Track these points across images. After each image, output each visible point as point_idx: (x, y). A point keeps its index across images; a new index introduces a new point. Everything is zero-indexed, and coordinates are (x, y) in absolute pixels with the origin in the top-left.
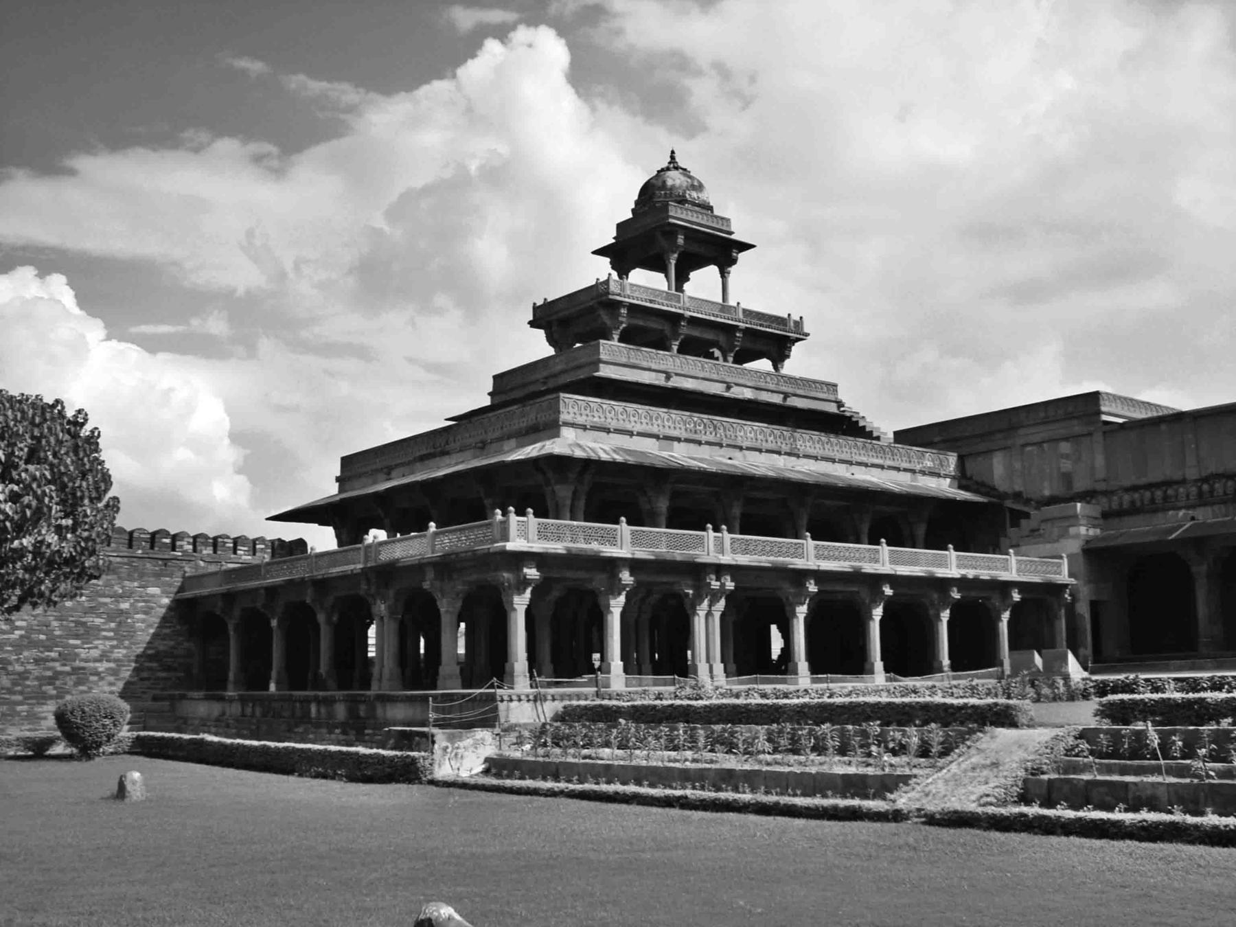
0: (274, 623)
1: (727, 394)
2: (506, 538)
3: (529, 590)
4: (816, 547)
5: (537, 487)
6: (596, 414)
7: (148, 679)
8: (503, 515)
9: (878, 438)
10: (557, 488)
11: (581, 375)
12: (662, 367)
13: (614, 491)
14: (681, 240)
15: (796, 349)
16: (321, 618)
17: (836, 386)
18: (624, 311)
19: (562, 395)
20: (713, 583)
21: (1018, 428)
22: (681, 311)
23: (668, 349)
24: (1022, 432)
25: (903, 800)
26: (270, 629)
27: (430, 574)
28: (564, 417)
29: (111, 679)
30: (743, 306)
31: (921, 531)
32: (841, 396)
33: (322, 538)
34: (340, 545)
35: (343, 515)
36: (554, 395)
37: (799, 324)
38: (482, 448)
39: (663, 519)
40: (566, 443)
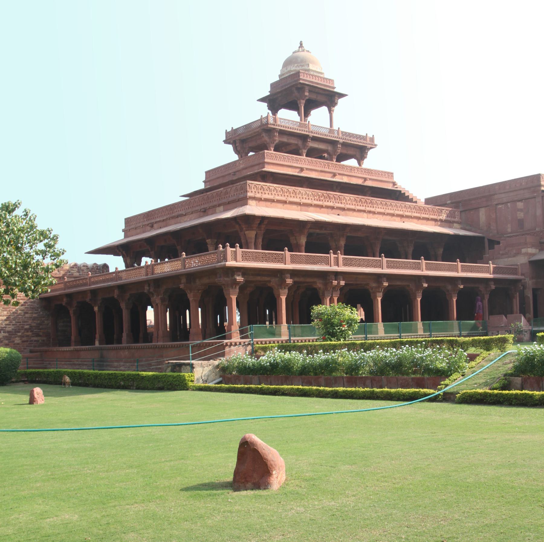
0: (96, 309)
1: (334, 180)
2: (225, 260)
3: (238, 287)
4: (387, 261)
5: (233, 232)
7: (27, 341)
8: (223, 248)
9: (416, 202)
10: (247, 232)
11: (256, 170)
13: (277, 234)
15: (370, 153)
16: (123, 306)
17: (392, 174)
19: (249, 182)
20: (334, 281)
21: (494, 195)
22: (307, 133)
23: (300, 155)
24: (496, 197)
25: (453, 384)
26: (94, 313)
27: (184, 280)
28: (249, 194)
29: (7, 342)
30: (341, 130)
31: (441, 251)
32: (395, 179)
33: (116, 263)
34: (127, 266)
35: (128, 250)
36: (244, 182)
37: (372, 139)
38: (205, 211)
39: (303, 248)
40: (252, 209)
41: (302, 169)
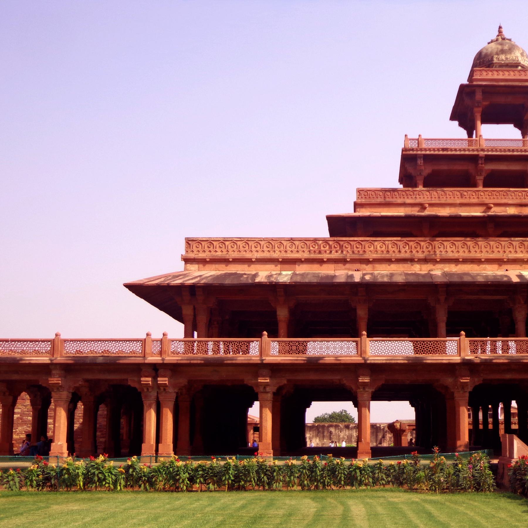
6: (218, 249)
12: (418, 201)
14: (479, 96)
18: (420, 162)
22: (475, 153)
41: (422, 207)
